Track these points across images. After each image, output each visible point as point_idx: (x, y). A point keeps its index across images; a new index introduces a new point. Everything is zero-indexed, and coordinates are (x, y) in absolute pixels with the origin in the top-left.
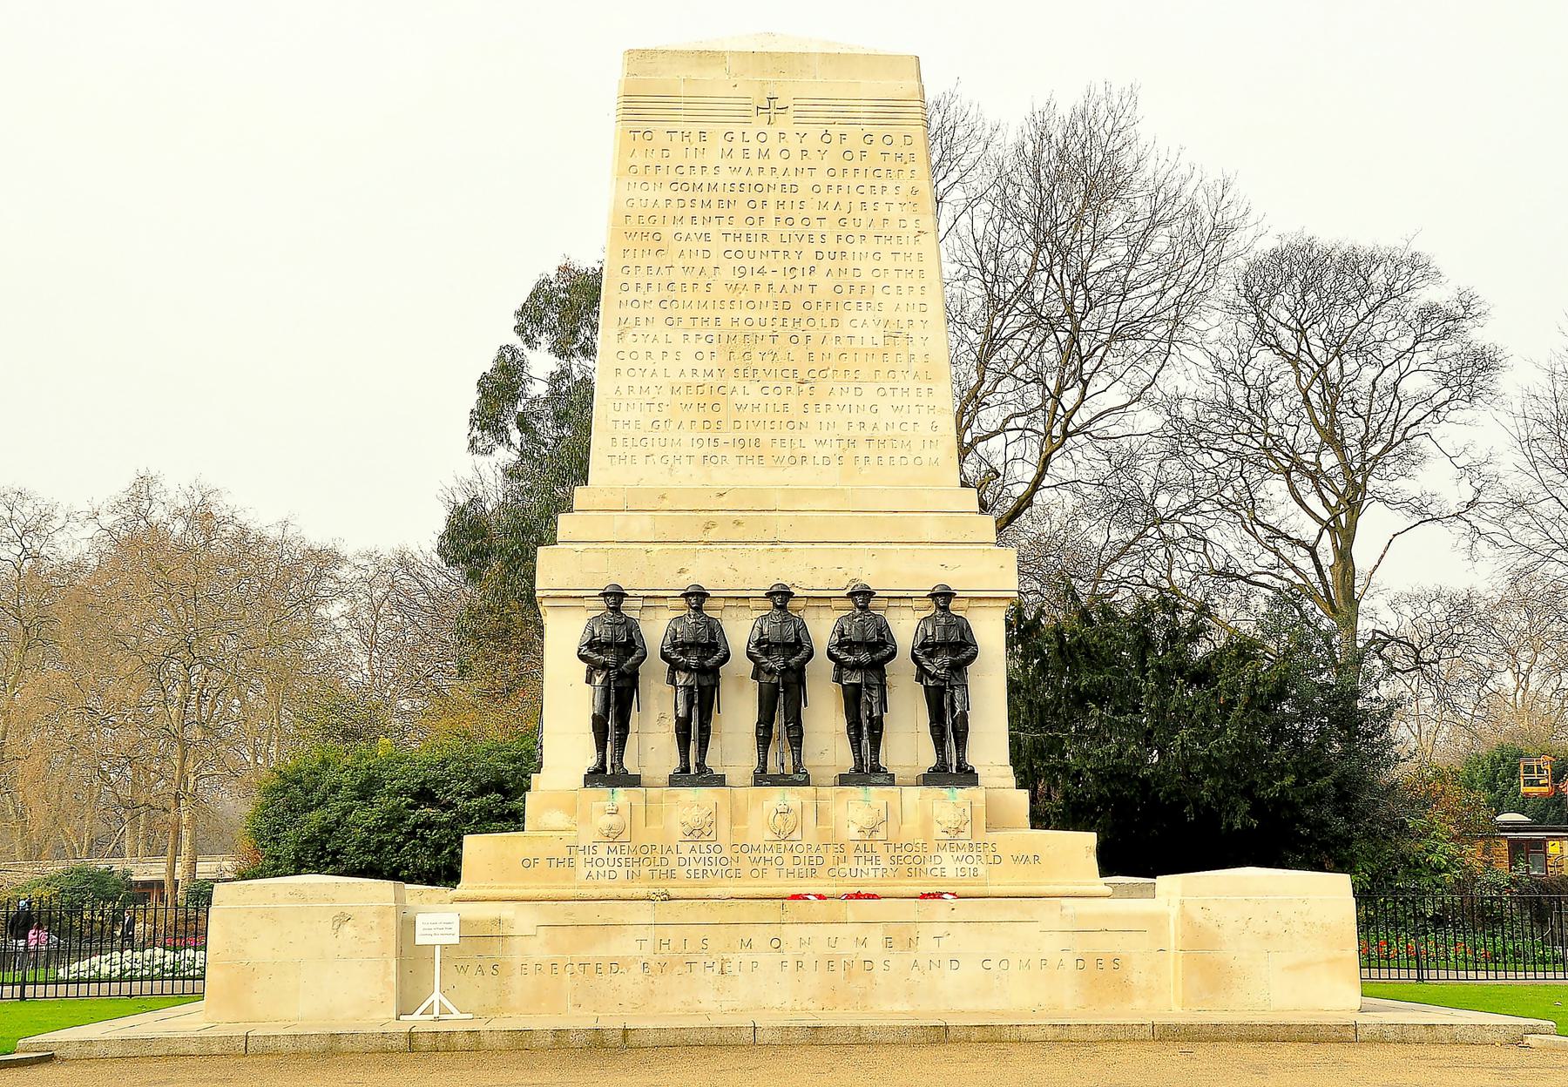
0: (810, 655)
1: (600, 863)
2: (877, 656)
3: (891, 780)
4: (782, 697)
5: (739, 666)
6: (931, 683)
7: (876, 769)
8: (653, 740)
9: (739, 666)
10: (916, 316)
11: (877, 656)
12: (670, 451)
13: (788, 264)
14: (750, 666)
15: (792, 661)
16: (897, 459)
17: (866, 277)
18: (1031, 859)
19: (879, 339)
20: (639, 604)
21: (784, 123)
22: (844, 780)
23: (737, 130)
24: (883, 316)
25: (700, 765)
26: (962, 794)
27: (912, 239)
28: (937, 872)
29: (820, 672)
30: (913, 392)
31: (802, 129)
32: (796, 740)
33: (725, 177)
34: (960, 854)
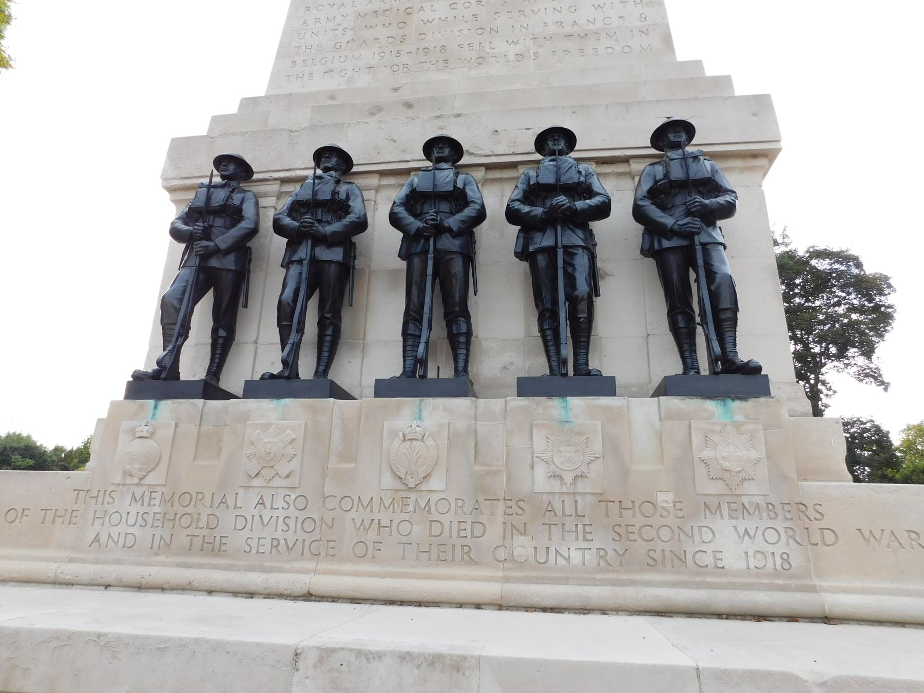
0: (481, 216)
1: (115, 518)
2: (580, 204)
3: (606, 386)
5: (383, 242)
6: (666, 244)
7: (582, 370)
8: (260, 348)
9: (383, 242)
11: (580, 204)
14: (397, 236)
15: (453, 222)
20: (274, 187)
22: (527, 387)
26: (741, 409)
28: (708, 560)
29: (497, 240)
32: (461, 340)
34: (749, 523)
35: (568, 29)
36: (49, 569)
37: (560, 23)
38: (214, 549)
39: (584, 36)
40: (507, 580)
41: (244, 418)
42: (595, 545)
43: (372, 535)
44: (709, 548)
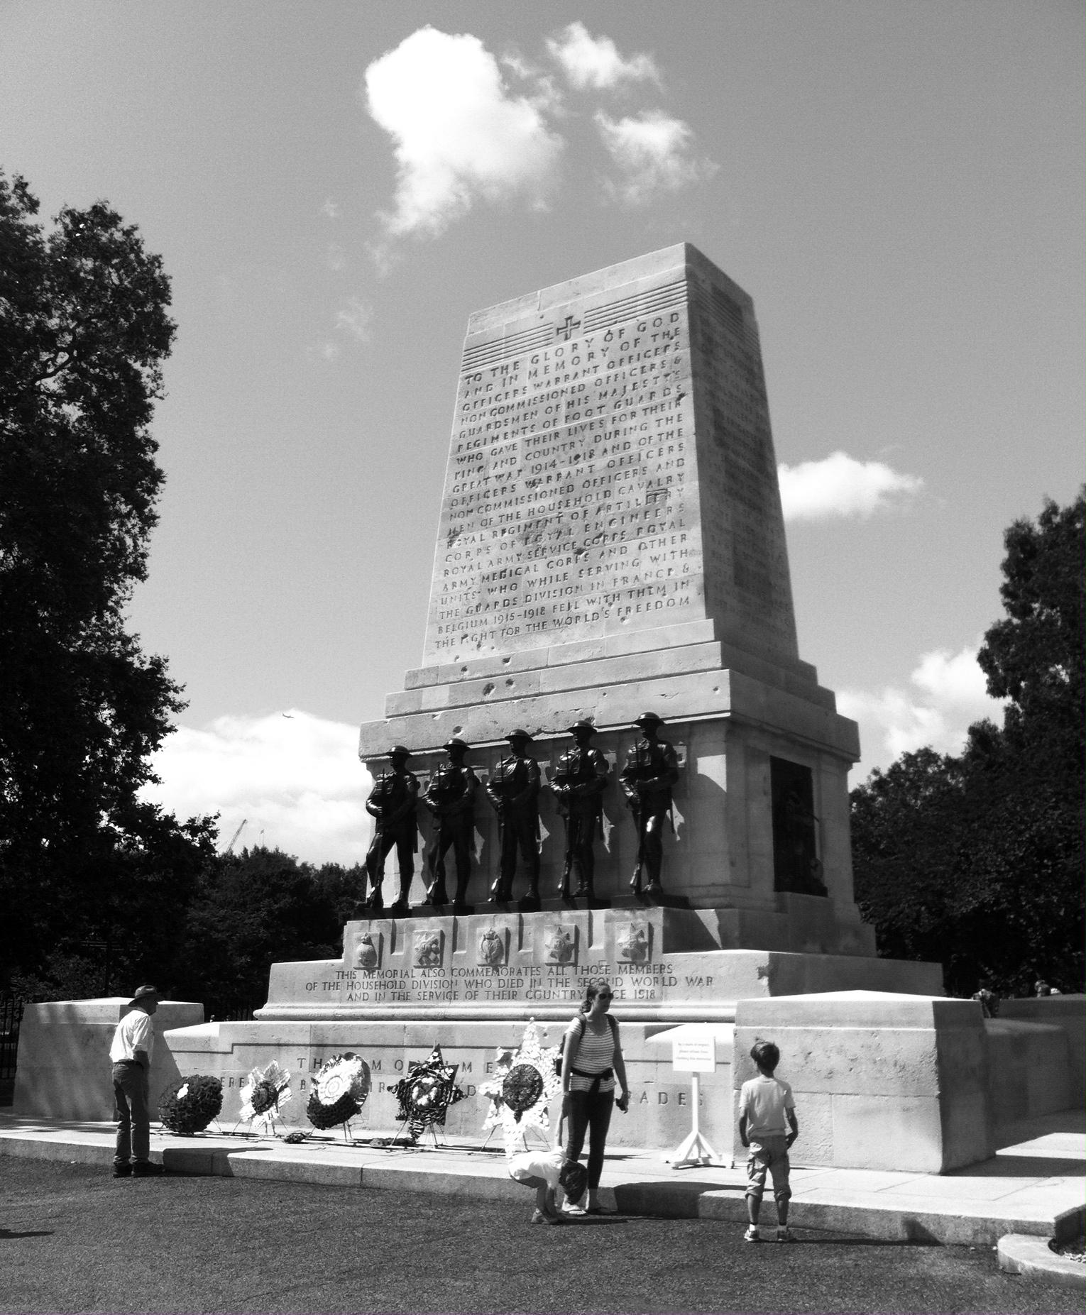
4: (518, 835)
10: (674, 471)
12: (478, 630)
13: (572, 453)
16: (653, 605)
17: (634, 450)
18: (704, 981)
19: (642, 500)
21: (578, 337)
23: (540, 352)
24: (648, 476)
25: (460, 894)
27: (673, 405)
30: (668, 542)
31: (589, 336)
33: (532, 393)
35: (630, 585)
36: (329, 1012)
37: (625, 579)
38: (404, 997)
39: (640, 592)
40: (530, 1007)
41: (412, 928)
42: (570, 989)
43: (474, 988)
44: (620, 988)
